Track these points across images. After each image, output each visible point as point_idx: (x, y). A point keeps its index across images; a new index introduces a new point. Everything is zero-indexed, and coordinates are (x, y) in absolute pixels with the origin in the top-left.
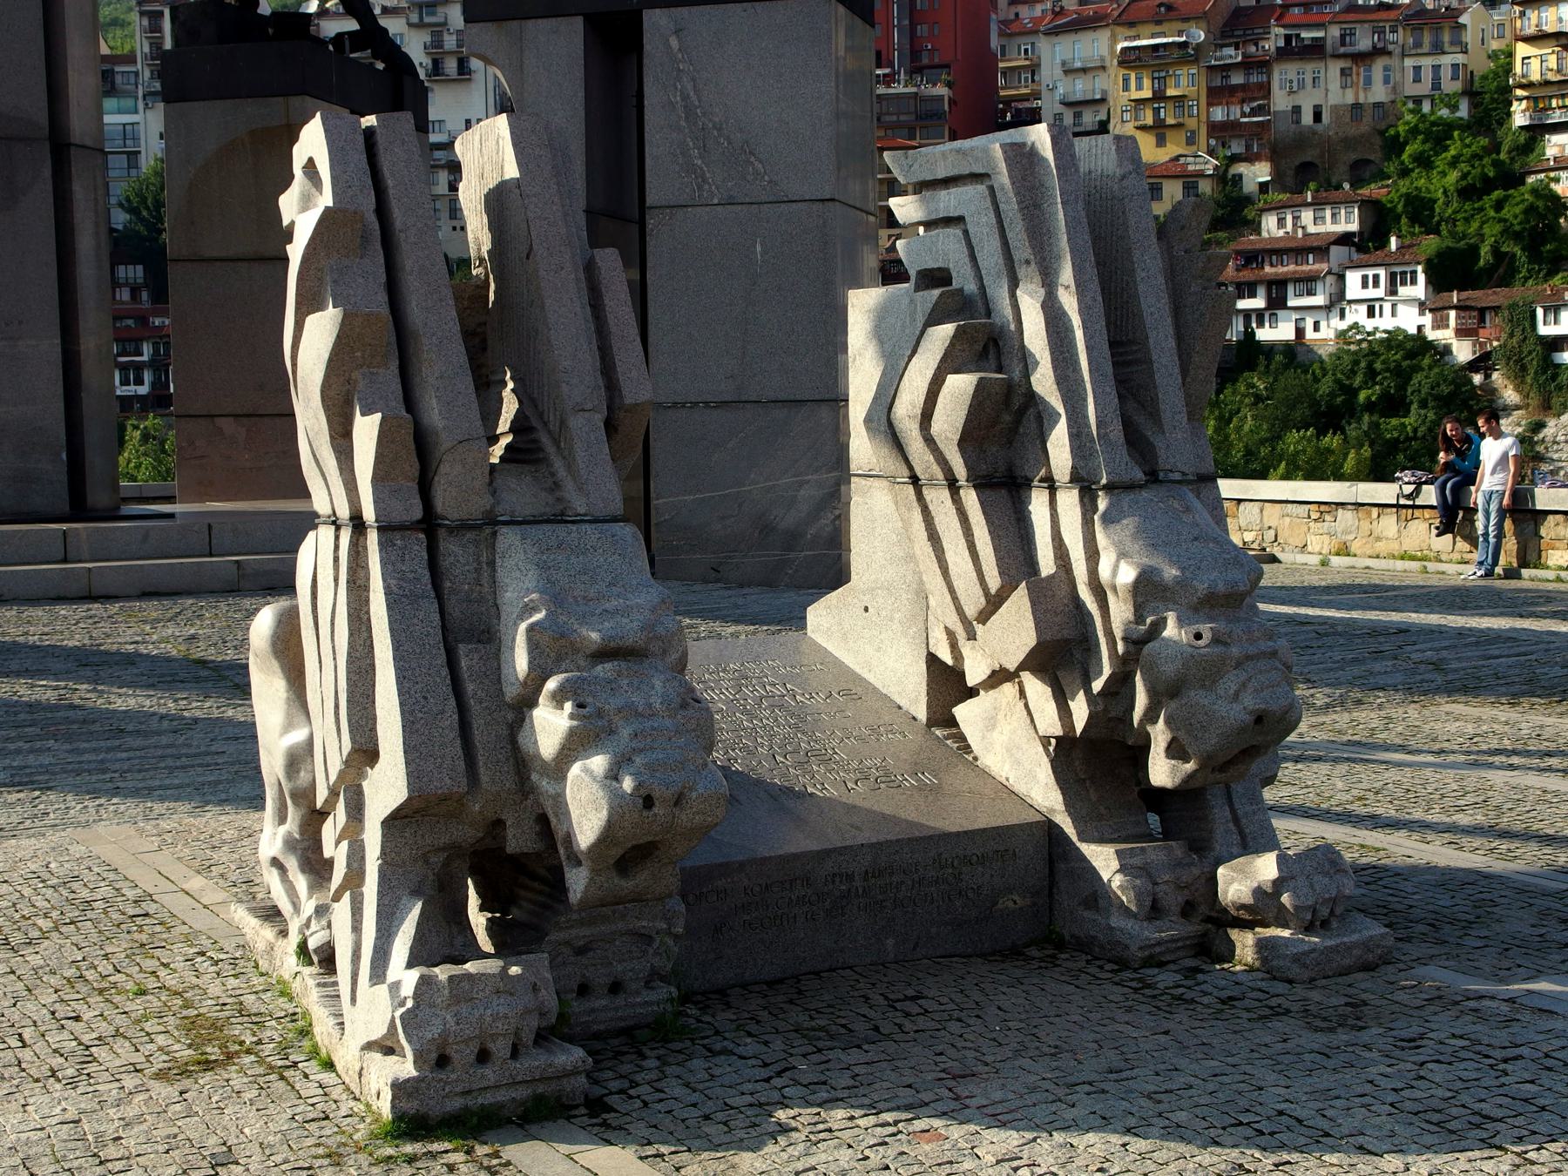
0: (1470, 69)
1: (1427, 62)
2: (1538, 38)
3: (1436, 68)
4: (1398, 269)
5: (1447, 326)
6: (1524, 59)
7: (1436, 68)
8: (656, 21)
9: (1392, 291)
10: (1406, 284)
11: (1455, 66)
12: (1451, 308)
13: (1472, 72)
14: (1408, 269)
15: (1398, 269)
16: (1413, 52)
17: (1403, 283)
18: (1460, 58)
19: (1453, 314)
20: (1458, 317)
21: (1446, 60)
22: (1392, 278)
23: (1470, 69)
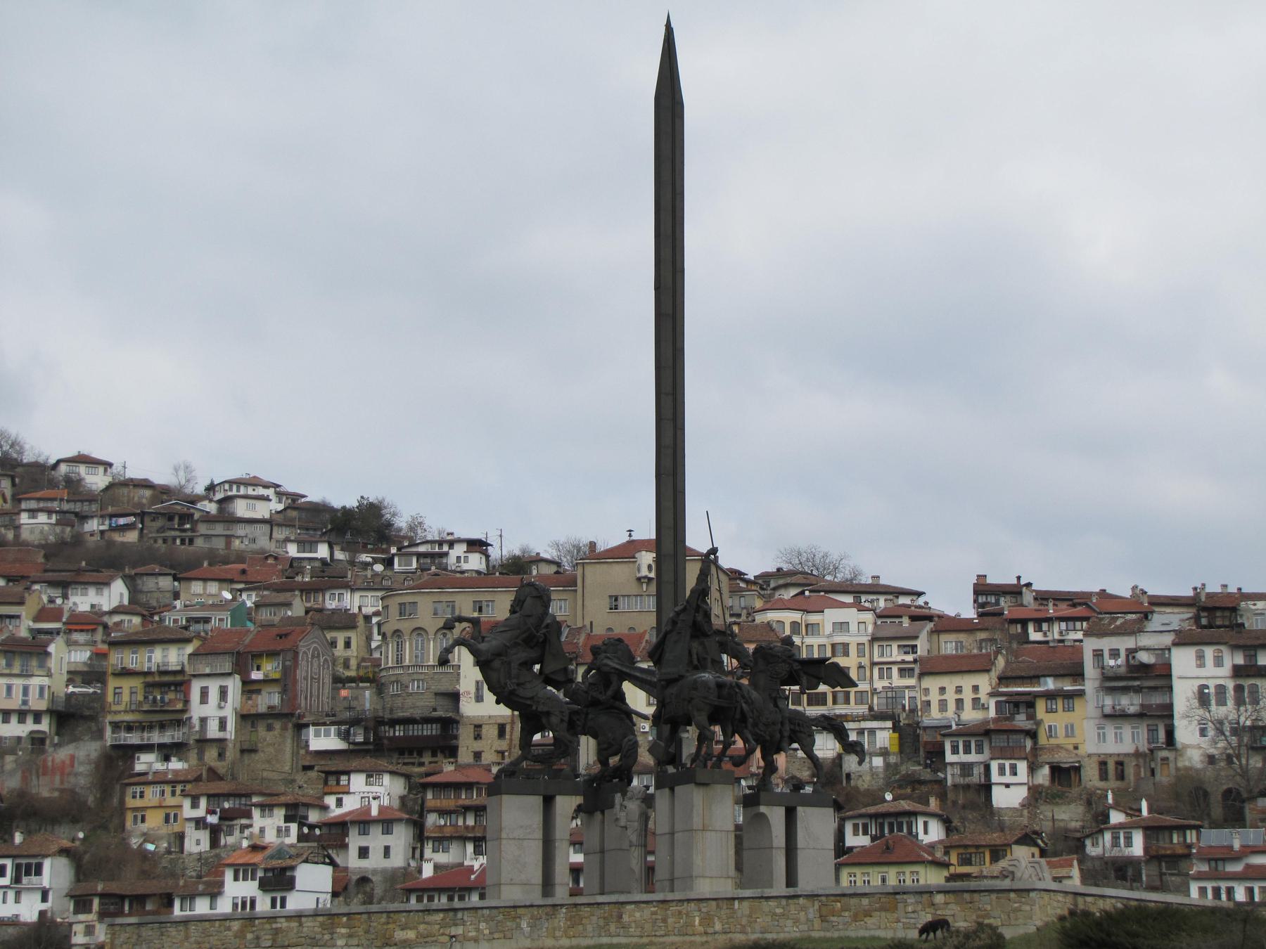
0: (52, 690)
1: (18, 683)
2: (126, 673)
3: (26, 690)
4: (24, 861)
5: (90, 911)
6: (115, 688)
7: (26, 690)
8: (800, 809)
9: (17, 880)
10: (30, 875)
11: (42, 689)
12: (95, 895)
13: (53, 693)
14: (34, 861)
15: (24, 861)
16: (7, 671)
17: (28, 873)
18: (45, 681)
19: (96, 902)
20: (101, 904)
21: (35, 682)
22: (18, 868)
23: (52, 690)
